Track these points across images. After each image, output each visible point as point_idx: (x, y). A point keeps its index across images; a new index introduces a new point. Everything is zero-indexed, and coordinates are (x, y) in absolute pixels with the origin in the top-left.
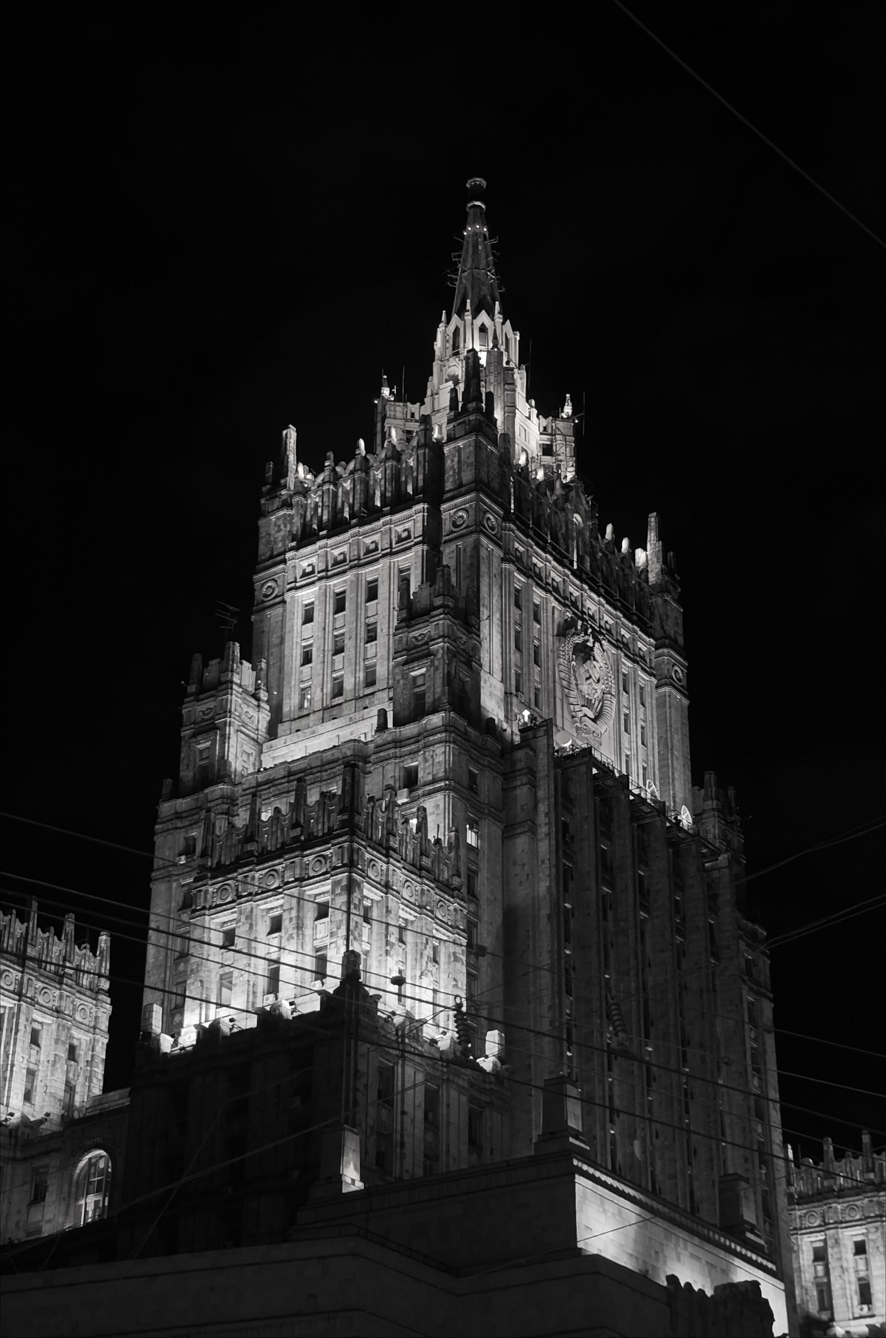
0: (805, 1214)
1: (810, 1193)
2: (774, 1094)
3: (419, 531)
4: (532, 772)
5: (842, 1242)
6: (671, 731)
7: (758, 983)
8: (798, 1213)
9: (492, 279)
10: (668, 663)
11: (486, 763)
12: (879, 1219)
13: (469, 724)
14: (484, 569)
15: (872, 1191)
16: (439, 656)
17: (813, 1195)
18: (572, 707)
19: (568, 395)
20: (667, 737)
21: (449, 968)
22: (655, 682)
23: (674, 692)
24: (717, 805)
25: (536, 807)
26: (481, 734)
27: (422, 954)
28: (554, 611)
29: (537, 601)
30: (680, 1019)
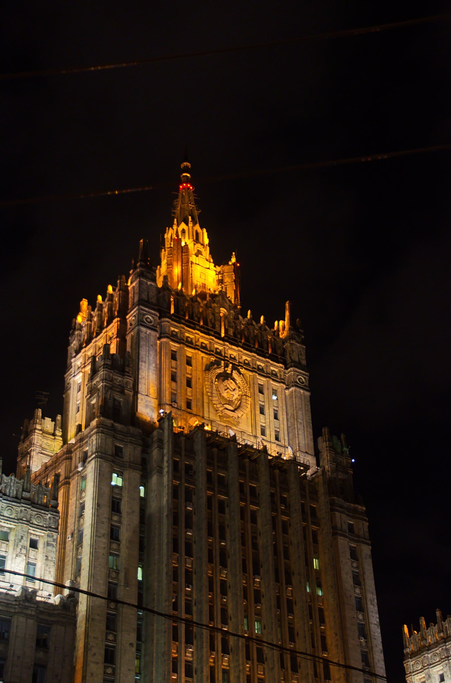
0: (414, 663)
1: (416, 650)
2: (371, 597)
3: (115, 333)
4: (161, 441)
5: (432, 676)
6: (296, 410)
7: (358, 536)
8: (412, 663)
9: (191, 207)
10: (294, 375)
11: (128, 441)
12: (447, 659)
13: (114, 421)
14: (142, 343)
15: (442, 643)
16: (101, 390)
17: (417, 651)
18: (215, 405)
19: (234, 253)
20: (294, 414)
21: (44, 550)
22: (285, 386)
23: (298, 389)
24: (329, 444)
25: (163, 458)
26: (126, 426)
27: (17, 545)
28: (201, 359)
29: (189, 355)
30: (283, 560)
